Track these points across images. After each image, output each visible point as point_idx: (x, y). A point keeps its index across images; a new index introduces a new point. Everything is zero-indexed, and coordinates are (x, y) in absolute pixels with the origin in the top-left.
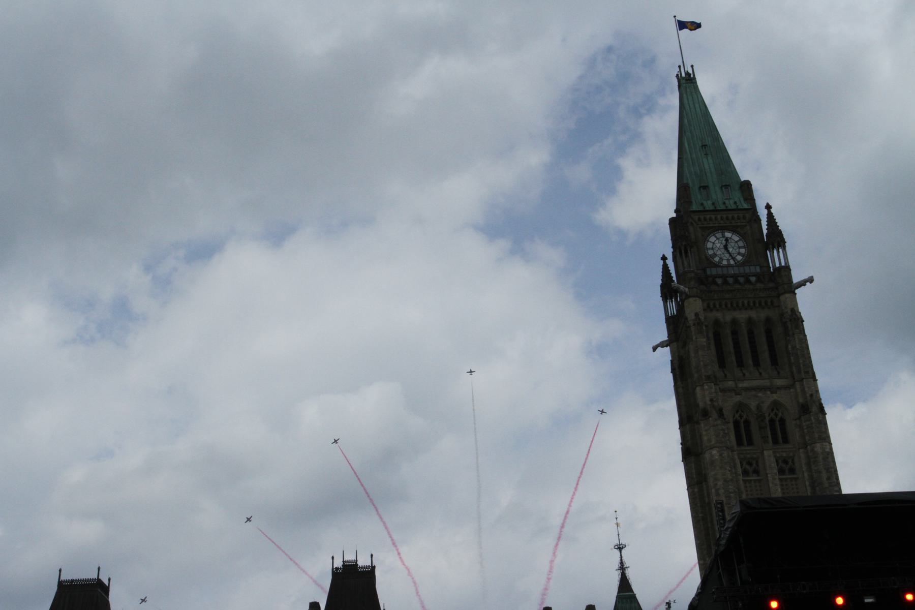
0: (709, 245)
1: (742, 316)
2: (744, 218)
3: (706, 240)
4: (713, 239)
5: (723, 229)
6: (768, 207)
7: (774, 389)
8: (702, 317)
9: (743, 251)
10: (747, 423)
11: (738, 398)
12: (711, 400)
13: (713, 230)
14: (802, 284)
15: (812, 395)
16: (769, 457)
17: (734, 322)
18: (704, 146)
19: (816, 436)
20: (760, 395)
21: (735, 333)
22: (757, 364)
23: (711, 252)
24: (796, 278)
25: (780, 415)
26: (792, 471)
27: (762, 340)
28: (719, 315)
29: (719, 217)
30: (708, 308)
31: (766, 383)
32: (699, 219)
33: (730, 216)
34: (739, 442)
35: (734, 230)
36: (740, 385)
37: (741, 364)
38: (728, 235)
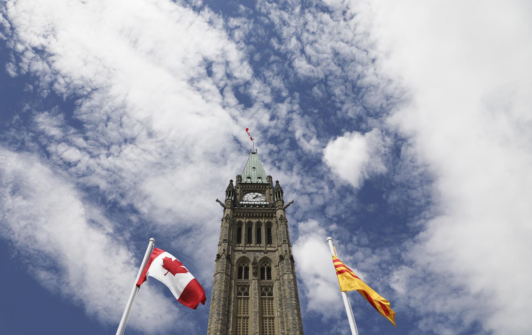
0: (246, 196)
3: (245, 194)
4: (248, 195)
5: (254, 191)
6: (277, 182)
10: (247, 269)
11: (244, 255)
12: (224, 250)
13: (249, 192)
14: (288, 205)
15: (286, 251)
18: (254, 168)
19: (285, 270)
20: (257, 254)
21: (249, 230)
22: (259, 241)
24: (285, 204)
26: (271, 294)
31: (263, 249)
32: (243, 187)
34: (240, 277)
36: (247, 249)
37: (249, 241)
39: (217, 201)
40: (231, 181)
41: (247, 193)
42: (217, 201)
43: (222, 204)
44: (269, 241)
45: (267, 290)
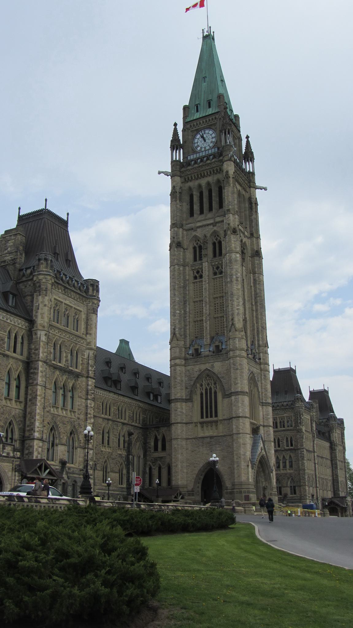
1: (203, 182)
2: (216, 118)
7: (214, 224)
8: (178, 189)
9: (214, 140)
10: (200, 247)
16: (206, 267)
17: (200, 186)
21: (201, 194)
22: (211, 209)
23: (196, 145)
25: (219, 238)
27: (215, 194)
28: (191, 184)
29: (201, 122)
30: (186, 181)
33: (207, 119)
35: (209, 127)
38: (207, 132)
39: (160, 173)
40: (175, 125)
41: (196, 135)
42: (160, 173)
43: (166, 174)
44: (221, 205)
45: (218, 268)
